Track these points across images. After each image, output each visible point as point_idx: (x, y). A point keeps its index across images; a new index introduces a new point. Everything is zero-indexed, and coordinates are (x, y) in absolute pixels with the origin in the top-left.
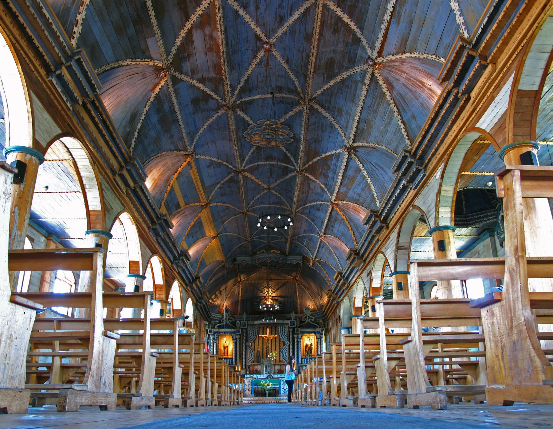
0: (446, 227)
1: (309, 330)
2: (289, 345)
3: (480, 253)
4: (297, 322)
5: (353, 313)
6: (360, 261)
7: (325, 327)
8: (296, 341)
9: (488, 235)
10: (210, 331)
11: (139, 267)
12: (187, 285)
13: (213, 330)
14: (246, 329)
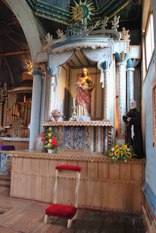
14: (7, 96)
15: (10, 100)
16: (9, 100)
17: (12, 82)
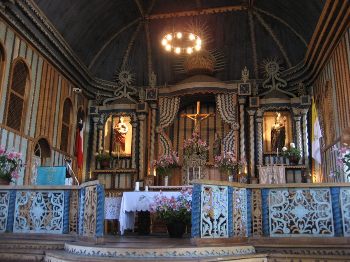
8: (252, 122)
10: (93, 110)
13: (97, 107)
14: (156, 102)
15: (165, 109)
16: (161, 109)
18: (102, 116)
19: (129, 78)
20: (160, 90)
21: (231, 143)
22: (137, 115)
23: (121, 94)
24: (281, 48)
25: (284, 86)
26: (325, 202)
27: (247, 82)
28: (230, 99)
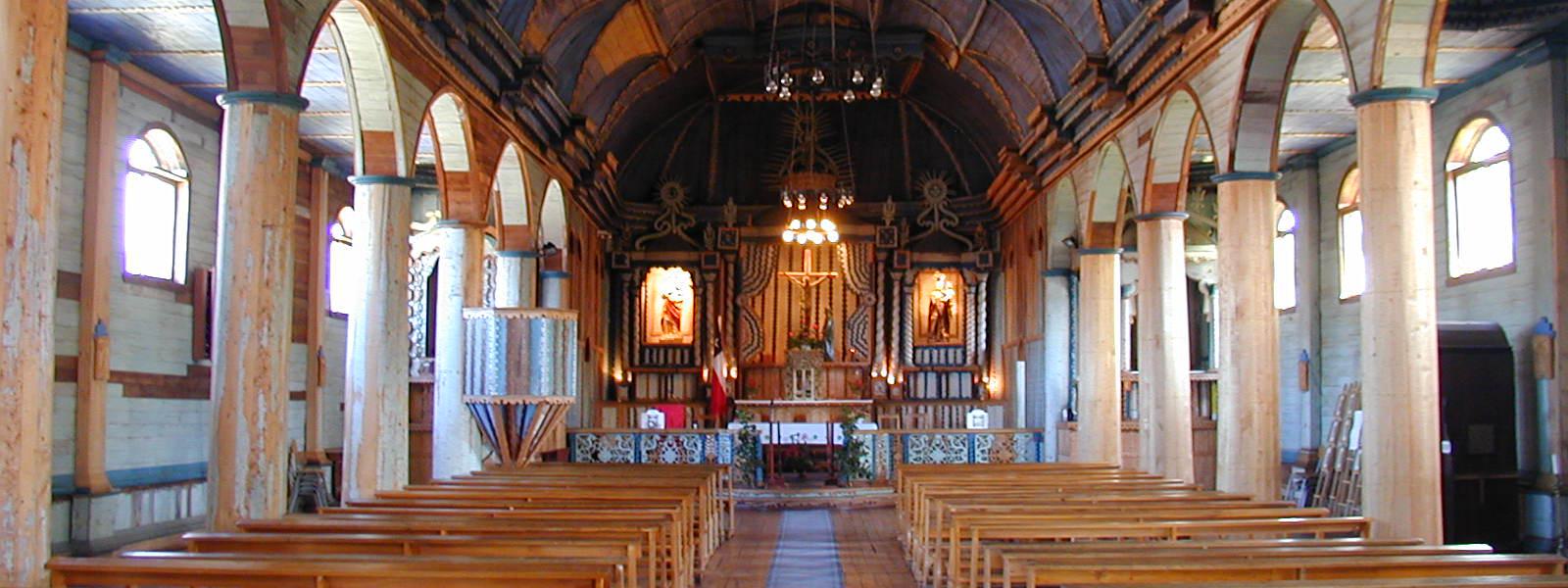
0: (1404, 93)
1: (939, 258)
2: (875, 308)
3: (1515, 99)
4: (900, 230)
5: (1086, 241)
6: (1115, 95)
7: (991, 246)
8: (896, 291)
9: (1546, 52)
10: (620, 260)
11: (394, 152)
12: (543, 149)
13: (627, 254)
14: (737, 253)
16: (744, 265)
17: (712, 181)
18: (637, 271)
19: (681, 192)
20: (743, 230)
21: (862, 326)
22: (701, 273)
23: (666, 227)
24: (952, 157)
25: (953, 224)
26: (961, 447)
27: (892, 224)
28: (863, 252)
